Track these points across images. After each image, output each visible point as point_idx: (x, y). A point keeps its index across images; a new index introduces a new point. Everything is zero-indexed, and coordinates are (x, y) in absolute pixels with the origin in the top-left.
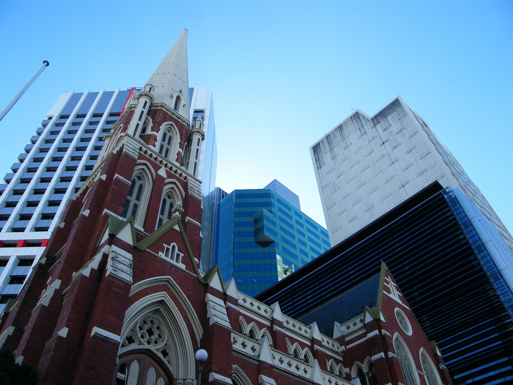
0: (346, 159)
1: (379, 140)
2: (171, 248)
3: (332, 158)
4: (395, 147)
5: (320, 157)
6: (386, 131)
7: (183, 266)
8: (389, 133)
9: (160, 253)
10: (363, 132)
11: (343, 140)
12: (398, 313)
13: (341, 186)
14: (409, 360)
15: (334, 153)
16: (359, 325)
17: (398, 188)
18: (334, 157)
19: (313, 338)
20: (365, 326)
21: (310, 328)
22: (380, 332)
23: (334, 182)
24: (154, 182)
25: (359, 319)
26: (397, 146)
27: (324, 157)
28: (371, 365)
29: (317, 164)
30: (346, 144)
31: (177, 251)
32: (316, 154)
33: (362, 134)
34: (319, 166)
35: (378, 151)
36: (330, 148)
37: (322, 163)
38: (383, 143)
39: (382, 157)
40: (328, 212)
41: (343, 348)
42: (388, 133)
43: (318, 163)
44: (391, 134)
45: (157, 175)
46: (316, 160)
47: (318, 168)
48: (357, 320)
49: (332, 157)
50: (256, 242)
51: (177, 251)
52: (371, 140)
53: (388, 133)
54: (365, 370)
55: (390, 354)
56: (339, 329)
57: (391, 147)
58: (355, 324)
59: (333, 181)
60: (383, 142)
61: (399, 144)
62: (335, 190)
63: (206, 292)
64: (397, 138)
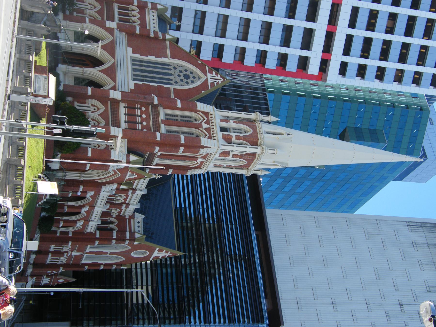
0: (403, 257)
1: (410, 302)
2: (134, 175)
3: (414, 242)
4: (387, 315)
5: (425, 229)
6: (418, 314)
7: (127, 178)
8: (413, 316)
9: (130, 173)
10: (431, 289)
11: (434, 262)
12: (146, 253)
13: (368, 240)
14: (115, 249)
15: (421, 246)
16: (137, 229)
17: (334, 299)
18: (415, 246)
19: (130, 205)
20: (134, 232)
21: (137, 204)
22: (128, 240)
23: (379, 235)
24: (193, 157)
25: (140, 230)
26: (387, 317)
27: (423, 234)
28: (112, 230)
29: (416, 222)
30: (426, 264)
32: (433, 225)
33: (429, 287)
34: (411, 225)
35: (393, 295)
36: (431, 244)
37: (414, 228)
38: (400, 305)
39: (383, 297)
40: (343, 218)
41: (127, 217)
42: (412, 315)
43: (417, 224)
44: (409, 317)
45: (198, 158)
46: (424, 223)
47: (409, 222)
48: (141, 229)
49: (415, 243)
50: (346, 128)
51: (134, 177)
52: (414, 294)
53: (412, 315)
54: (112, 226)
55: (114, 242)
56: (139, 217)
57: (391, 310)
58: (139, 227)
59: (381, 235)
60: (402, 305)
61: (390, 320)
62: (367, 233)
63: (118, 184)
64: (399, 321)
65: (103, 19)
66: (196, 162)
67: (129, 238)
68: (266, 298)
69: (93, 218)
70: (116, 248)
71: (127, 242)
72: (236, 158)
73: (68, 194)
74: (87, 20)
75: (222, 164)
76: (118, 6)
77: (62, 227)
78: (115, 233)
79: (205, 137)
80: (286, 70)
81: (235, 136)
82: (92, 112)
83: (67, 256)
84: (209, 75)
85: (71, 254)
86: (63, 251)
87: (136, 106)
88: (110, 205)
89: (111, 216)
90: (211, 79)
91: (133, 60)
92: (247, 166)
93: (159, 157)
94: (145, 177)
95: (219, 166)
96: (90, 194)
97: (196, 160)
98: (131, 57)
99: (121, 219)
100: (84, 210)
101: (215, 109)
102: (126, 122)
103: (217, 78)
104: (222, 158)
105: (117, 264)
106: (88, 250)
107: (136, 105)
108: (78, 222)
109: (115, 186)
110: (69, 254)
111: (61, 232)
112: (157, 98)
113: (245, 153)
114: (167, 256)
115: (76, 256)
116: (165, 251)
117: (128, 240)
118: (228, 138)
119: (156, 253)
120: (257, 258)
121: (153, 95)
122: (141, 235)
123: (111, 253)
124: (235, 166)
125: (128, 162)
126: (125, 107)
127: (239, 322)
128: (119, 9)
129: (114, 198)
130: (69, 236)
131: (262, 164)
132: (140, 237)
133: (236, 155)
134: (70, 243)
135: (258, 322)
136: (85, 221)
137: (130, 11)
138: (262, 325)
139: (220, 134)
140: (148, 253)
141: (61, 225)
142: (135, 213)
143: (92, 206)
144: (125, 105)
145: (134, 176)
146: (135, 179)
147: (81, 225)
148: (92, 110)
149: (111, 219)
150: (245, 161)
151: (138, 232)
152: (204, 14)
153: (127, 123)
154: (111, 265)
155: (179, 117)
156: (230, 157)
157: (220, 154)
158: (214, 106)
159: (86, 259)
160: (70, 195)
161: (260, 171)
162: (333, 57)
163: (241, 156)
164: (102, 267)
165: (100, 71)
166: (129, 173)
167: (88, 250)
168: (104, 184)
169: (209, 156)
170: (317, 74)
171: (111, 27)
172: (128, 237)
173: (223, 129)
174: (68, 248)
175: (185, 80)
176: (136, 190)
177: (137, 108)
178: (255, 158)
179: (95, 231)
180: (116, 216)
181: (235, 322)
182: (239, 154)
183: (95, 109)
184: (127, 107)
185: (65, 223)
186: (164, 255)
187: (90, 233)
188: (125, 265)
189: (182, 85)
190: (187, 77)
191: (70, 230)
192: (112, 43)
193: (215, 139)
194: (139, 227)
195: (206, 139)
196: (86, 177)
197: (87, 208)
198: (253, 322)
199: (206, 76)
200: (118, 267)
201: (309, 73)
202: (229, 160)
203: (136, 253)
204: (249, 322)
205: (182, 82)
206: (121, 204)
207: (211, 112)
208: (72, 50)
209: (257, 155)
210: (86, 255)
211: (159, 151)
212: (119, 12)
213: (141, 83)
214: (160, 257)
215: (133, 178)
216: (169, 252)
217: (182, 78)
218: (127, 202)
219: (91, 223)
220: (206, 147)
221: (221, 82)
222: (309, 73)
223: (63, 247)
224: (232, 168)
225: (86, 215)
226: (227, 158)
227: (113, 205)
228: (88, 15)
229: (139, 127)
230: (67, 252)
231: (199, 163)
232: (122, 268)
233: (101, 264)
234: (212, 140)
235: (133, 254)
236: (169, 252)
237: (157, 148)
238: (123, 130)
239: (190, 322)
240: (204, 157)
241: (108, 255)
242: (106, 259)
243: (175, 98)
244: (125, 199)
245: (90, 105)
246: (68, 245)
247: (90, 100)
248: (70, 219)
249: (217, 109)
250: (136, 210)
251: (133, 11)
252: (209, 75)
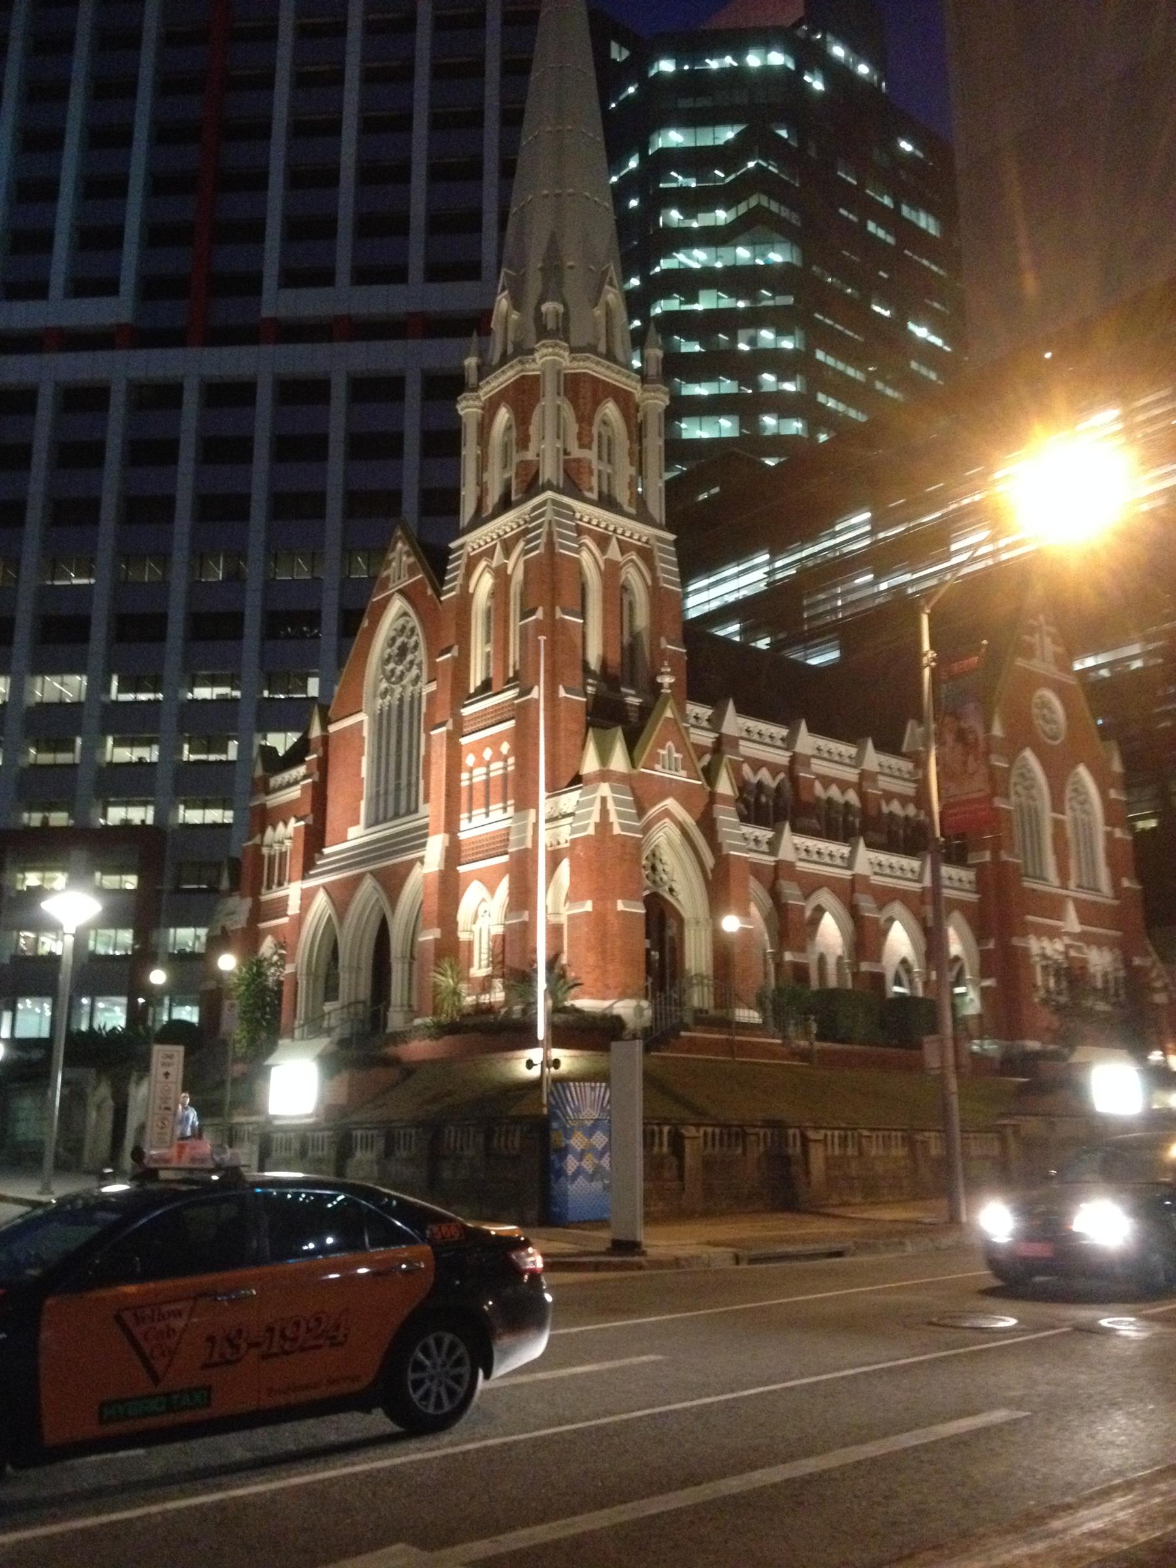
51: (676, 755)
72: (591, 436)
125: (604, 775)
133: (580, 437)
142: (904, 749)
165: (381, 909)
177: (471, 779)
182: (573, 428)
186: (1048, 640)
208: (364, 1002)
226: (595, 465)
241: (1067, 818)
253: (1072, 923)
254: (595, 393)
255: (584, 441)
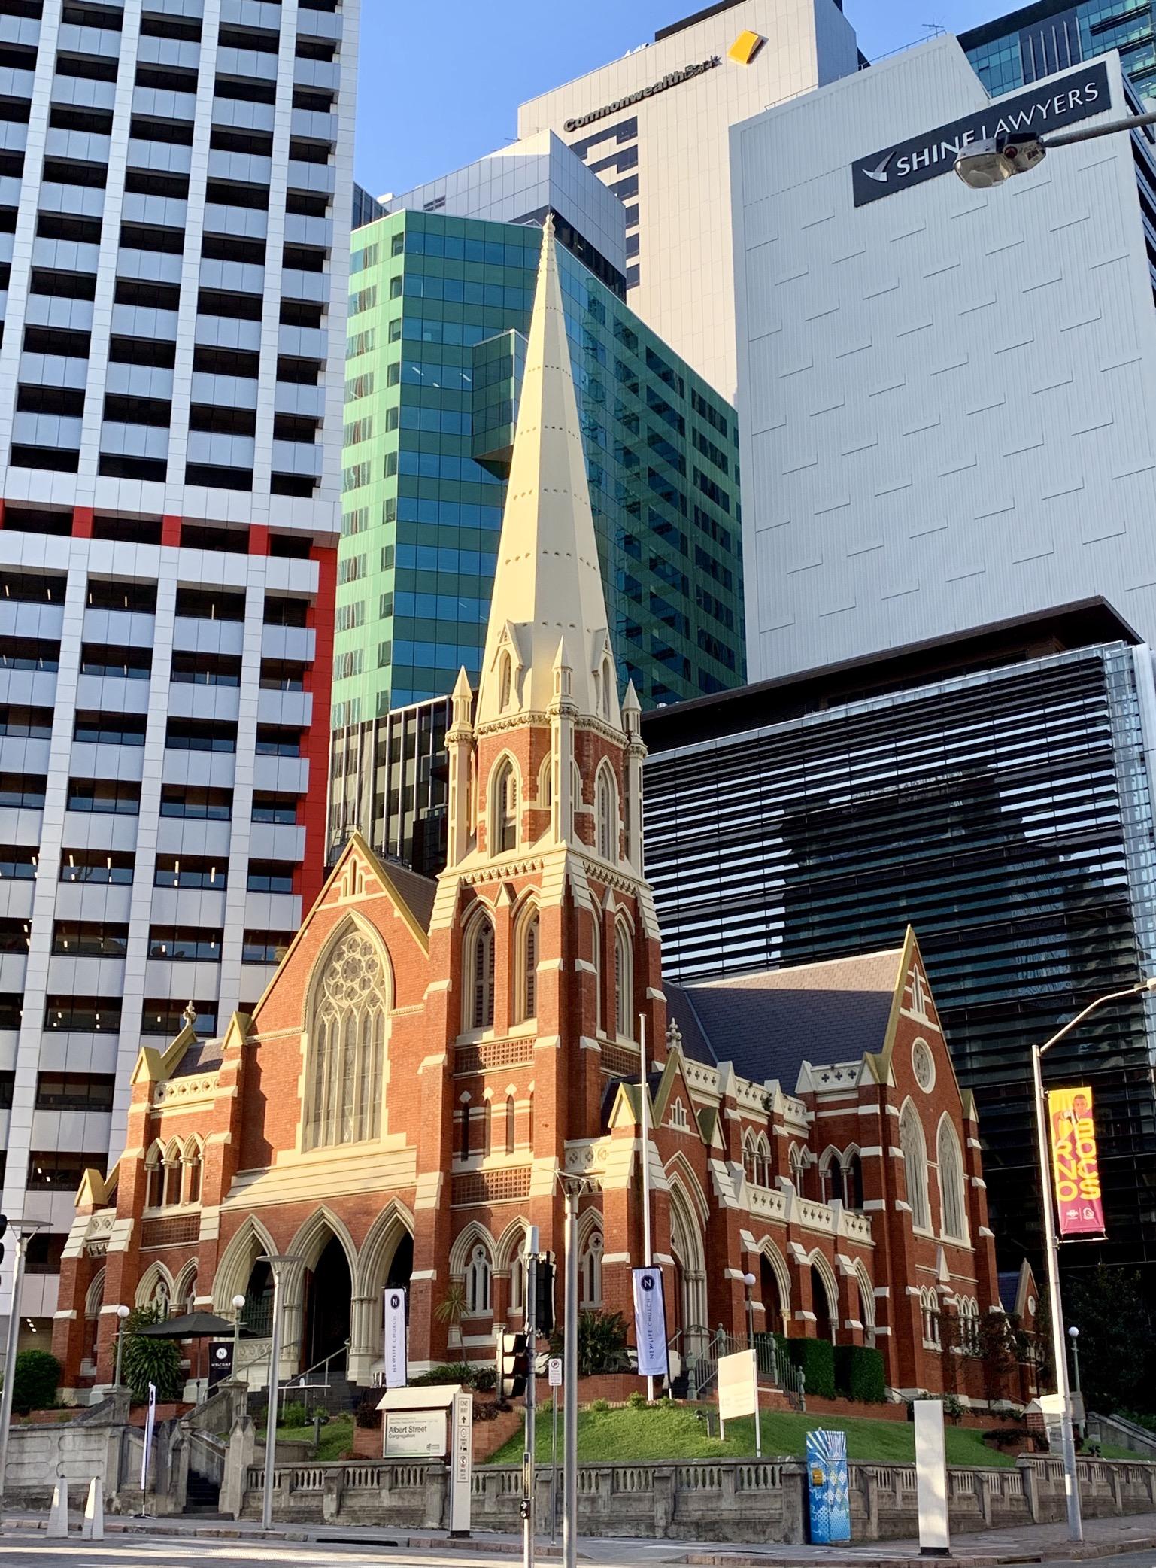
7: (686, 1129)
9: (671, 1122)
12: (919, 1047)
20: (858, 1089)
22: (883, 1109)
24: (602, 925)
28: (856, 1161)
31: (681, 1109)
41: (811, 1116)
45: (604, 911)
51: (681, 1109)
54: (844, 1165)
58: (839, 1077)
63: (709, 1156)
65: (194, 1251)
66: (619, 916)
67: (878, 1106)
68: (1022, 658)
69: (825, 1226)
70: (914, 1143)
71: (891, 1110)
73: (758, 1312)
74: (200, 1301)
75: (618, 834)
76: (150, 1205)
77: (863, 1321)
78: (865, 1152)
79: (538, 896)
80: (312, 658)
81: (525, 799)
82: (491, 1262)
83: (952, 1296)
84: (343, 901)
85: (945, 1283)
86: (937, 1309)
87: (460, 1120)
88: (778, 1174)
89: (814, 1167)
90: (354, 893)
91: (316, 1145)
92: (617, 757)
93: (612, 1036)
94: (678, 1071)
95: (626, 842)
96: (750, 1243)
97: (614, 915)
98: (304, 1150)
99: (818, 1136)
100: (804, 1258)
101: (447, 870)
102: (510, 1148)
103: (349, 875)
104: (596, 833)
105: (966, 1135)
106: (929, 1232)
107: (455, 1121)
108: (842, 1274)
109: (718, 1165)
110: (947, 1289)
111: (881, 1321)
112: (427, 1058)
113: (575, 765)
114: (924, 981)
115: (950, 1268)
116: (907, 988)
117: (883, 1109)
118: (535, 824)
119: (918, 1015)
120: (903, 697)
121: (420, 1071)
122: (866, 1067)
123: (931, 1157)
124: (620, 793)
126: (465, 1158)
127: (1107, 735)
128: (160, 1204)
129: (758, 1164)
130: (888, 1295)
131: (607, 709)
132: (871, 1070)
133: (583, 794)
134: (912, 1290)
135: (1101, 677)
136: (836, 1251)
137: (162, 1167)
138: (1109, 663)
139: (522, 849)
140: (918, 1040)
141: (857, 1324)
143: (789, 1232)
144: (457, 1157)
145: (678, 1106)
146: (688, 1103)
147: (852, 1260)
148: (483, 1260)
149: (824, 1166)
150: (601, 764)
151: (855, 1077)
152: (157, 932)
153: (516, 1146)
154: (968, 1152)
155: (480, 983)
156: (594, 810)
157: (585, 844)
158: (437, 876)
159: (958, 1234)
160: (758, 1306)
161: (627, 715)
162: (259, 519)
163: (587, 776)
164: (980, 1183)
166: (672, 1124)
167: (929, 1232)
168: (713, 1200)
169: (595, 878)
170: (316, 564)
171: (216, 1223)
172: (875, 1109)
173: (505, 839)
174: (929, 1294)
175: (363, 973)
176: (724, 1095)
177: (466, 1116)
178: (588, 732)
179: (867, 1213)
180: (812, 1152)
181: (1107, 746)
182: (580, 783)
183: (480, 1254)
184: (465, 1149)
185: (851, 1314)
186: (920, 988)
187: (875, 1230)
188: (965, 1111)
189: (383, 983)
190: (352, 969)
191: (870, 1294)
192: (270, 1213)
193: (542, 866)
194: (839, 1077)
195: (543, 892)
196: (697, 1263)
197: (798, 1248)
198: (1102, 691)
199: (345, 907)
200: (974, 1130)
201: (315, 589)
202: (603, 812)
203: (924, 1078)
204: (1104, 705)
205: (372, 985)
206: (773, 1139)
207: (455, 880)
209: (579, 728)
210: (944, 1238)
211: (593, 1036)
212: (169, 1202)
213: (384, 1113)
214: (929, 1000)
215: (685, 1111)
216: (910, 973)
217: (356, 985)
218: (764, 1121)
219: (841, 1231)
220: (568, 888)
221: (361, 859)
222: (315, 589)
223: (925, 1311)
224: (627, 800)
225: (817, 1249)
227: (777, 1164)
228: (189, 1300)
229: (522, 1106)
230: (941, 1296)
231: (622, 905)
232: (973, 1117)
233: (969, 1184)
234: (546, 871)
235: (928, 1089)
236: (910, 973)
237: (586, 1042)
238: (537, 1156)
239: (1123, 887)
240: (602, 893)
241: (937, 1166)
242: (952, 1171)
243: (424, 1001)
244: (757, 1127)
245: (469, 1270)
246: (917, 1297)
247: (457, 1268)
248: (836, 1297)
249: (445, 865)
250: (788, 1089)
251: (160, 1156)
252: (343, 901)
253: (944, 1275)
254: (596, 751)
255: (587, 798)
